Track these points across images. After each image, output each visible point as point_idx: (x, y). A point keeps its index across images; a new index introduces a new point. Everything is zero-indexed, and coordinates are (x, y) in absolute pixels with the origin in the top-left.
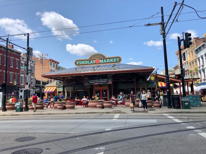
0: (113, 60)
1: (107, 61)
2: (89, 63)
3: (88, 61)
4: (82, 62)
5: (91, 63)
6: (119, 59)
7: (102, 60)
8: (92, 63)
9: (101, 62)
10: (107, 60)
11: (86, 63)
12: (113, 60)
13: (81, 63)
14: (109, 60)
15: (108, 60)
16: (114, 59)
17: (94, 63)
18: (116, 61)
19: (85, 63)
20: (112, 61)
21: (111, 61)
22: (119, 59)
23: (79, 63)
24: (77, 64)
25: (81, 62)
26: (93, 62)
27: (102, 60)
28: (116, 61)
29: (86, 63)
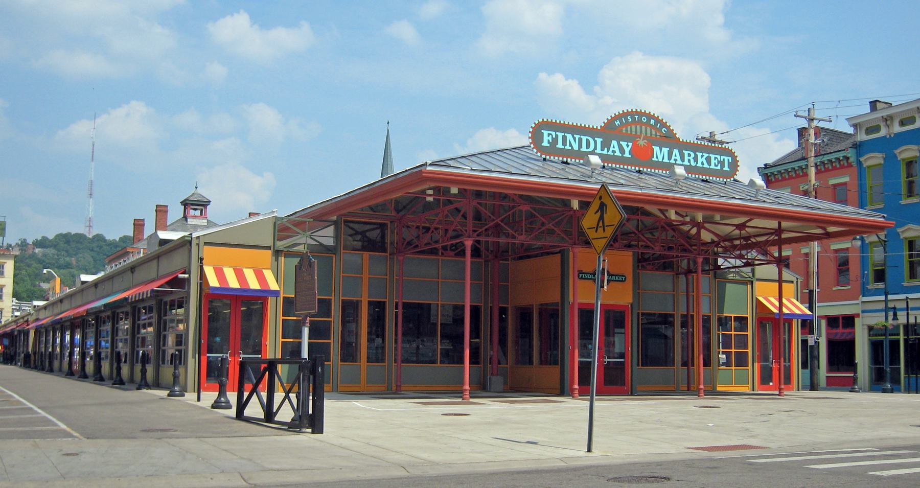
2: (605, 152)
3: (599, 140)
4: (569, 137)
5: (610, 153)
7: (665, 150)
8: (618, 154)
9: (660, 160)
10: (686, 153)
11: (588, 146)
13: (564, 143)
15: (689, 155)
16: (713, 156)
17: (627, 155)
18: (719, 168)
20: (702, 163)
22: (730, 159)
23: (555, 140)
24: (545, 144)
25: (564, 138)
27: (665, 150)
28: (719, 168)
29: (588, 146)
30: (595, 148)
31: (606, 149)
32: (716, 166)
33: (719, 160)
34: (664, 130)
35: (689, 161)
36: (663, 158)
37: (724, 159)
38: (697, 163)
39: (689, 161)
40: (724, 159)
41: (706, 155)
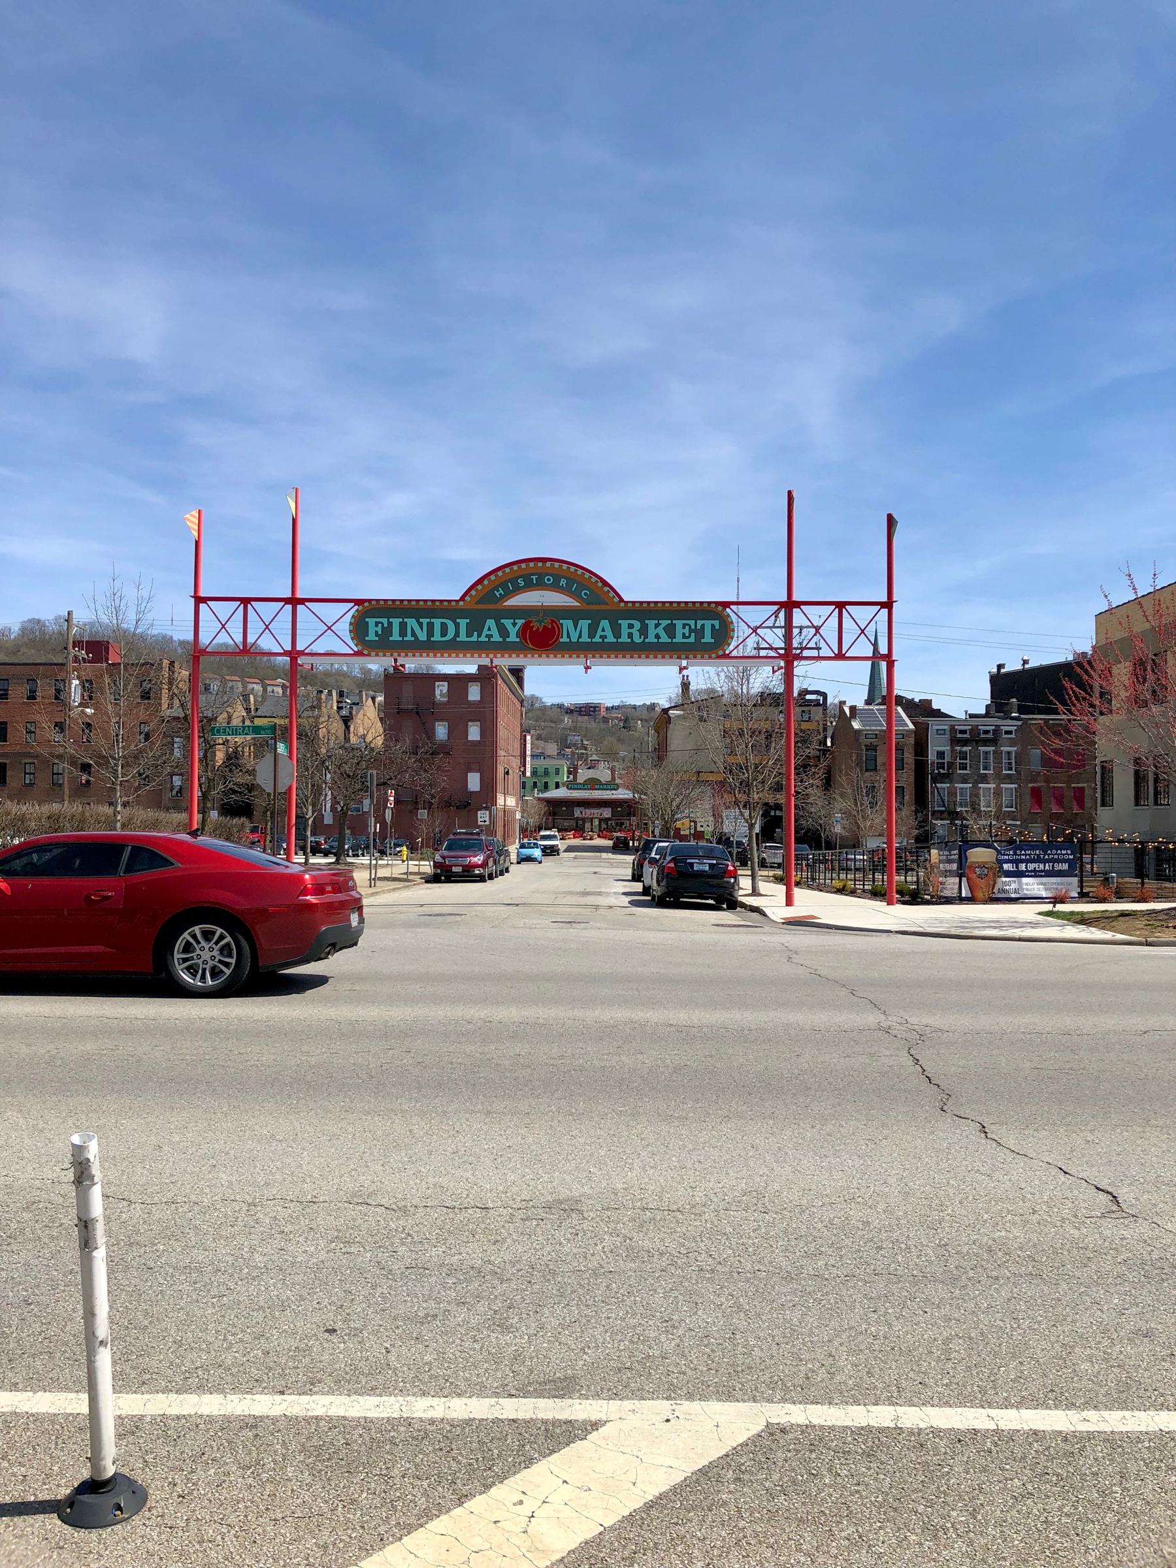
0: (670, 631)
1: (625, 631)
2: (474, 638)
3: (463, 623)
4: (411, 622)
5: (483, 639)
6: (716, 623)
7: (584, 624)
9: (574, 640)
10: (624, 623)
12: (670, 631)
14: (637, 624)
15: (631, 626)
16: (679, 623)
17: (513, 638)
18: (692, 639)
19: (437, 637)
20: (657, 636)
21: (651, 639)
22: (716, 623)
23: (388, 631)
24: (371, 637)
25: (403, 627)
26: (504, 632)
27: (584, 624)
28: (692, 639)
30: (457, 634)
31: (476, 633)
32: (684, 636)
33: (693, 627)
34: (585, 594)
35: (630, 635)
36: (580, 636)
37: (703, 626)
38: (646, 637)
39: (630, 635)
40: (703, 626)
41: (664, 623)
